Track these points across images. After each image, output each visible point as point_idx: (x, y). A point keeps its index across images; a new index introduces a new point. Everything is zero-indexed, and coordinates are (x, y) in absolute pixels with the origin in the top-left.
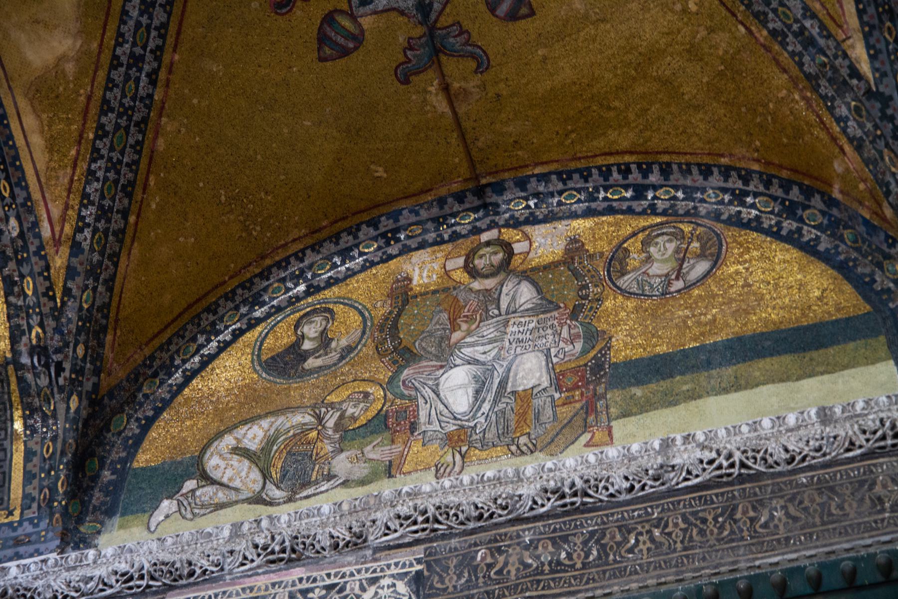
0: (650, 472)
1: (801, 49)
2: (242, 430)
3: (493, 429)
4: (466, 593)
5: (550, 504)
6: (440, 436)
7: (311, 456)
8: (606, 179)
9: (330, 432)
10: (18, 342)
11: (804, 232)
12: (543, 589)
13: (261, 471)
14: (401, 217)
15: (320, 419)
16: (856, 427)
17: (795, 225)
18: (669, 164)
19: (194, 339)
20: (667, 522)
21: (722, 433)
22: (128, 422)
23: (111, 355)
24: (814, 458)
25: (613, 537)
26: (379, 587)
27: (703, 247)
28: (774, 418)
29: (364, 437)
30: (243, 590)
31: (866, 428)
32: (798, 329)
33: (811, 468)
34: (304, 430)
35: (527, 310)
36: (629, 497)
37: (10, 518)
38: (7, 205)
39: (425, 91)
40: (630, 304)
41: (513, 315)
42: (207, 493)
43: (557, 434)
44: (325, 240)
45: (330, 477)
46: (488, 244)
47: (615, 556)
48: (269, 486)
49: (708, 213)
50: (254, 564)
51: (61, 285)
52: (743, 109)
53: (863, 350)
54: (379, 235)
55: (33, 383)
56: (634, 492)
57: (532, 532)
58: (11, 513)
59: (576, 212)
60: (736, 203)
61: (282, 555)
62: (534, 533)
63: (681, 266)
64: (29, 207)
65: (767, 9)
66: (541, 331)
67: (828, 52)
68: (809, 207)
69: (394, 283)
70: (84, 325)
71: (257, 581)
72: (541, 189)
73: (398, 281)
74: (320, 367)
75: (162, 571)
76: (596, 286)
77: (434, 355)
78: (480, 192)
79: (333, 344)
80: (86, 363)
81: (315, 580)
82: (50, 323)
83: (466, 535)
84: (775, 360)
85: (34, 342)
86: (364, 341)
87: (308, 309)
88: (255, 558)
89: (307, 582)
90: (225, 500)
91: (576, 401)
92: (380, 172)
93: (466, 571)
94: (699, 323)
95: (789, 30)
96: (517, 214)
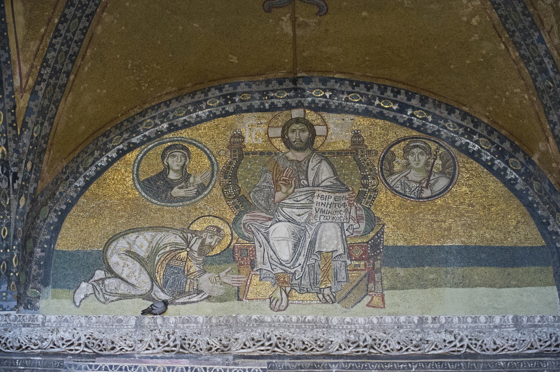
0: (414, 342)
1: (537, 72)
2: (132, 236)
3: (307, 278)
6: (271, 275)
8: (382, 93)
9: (196, 255)
14: (239, 87)
15: (188, 243)
16: (536, 337)
17: (503, 165)
18: (427, 98)
19: (92, 154)
21: (456, 320)
22: (50, 212)
23: (46, 168)
24: (509, 350)
27: (443, 165)
28: (487, 317)
29: (219, 264)
30: (148, 367)
31: (542, 339)
32: (501, 248)
33: (506, 356)
35: (327, 187)
36: (397, 354)
39: (280, 19)
40: (397, 200)
41: (317, 188)
42: (112, 283)
43: (349, 292)
44: (186, 95)
45: (199, 292)
46: (297, 120)
48: (156, 288)
50: (155, 351)
51: (22, 118)
52: (488, 87)
53: (539, 274)
54: (221, 95)
56: (401, 351)
57: (337, 366)
59: (357, 109)
60: (466, 136)
61: (174, 349)
62: (338, 368)
63: (429, 177)
64: (8, 64)
65: (522, 43)
67: (554, 81)
68: (514, 157)
69: (232, 137)
70: (33, 148)
71: (157, 363)
72: (337, 87)
73: (233, 136)
75: (93, 344)
76: (373, 179)
77: (264, 208)
78: (295, 81)
79: (191, 180)
80: (31, 175)
82: (12, 145)
83: (294, 359)
84: (487, 269)
86: (213, 182)
87: (169, 144)
88: (156, 347)
91: (363, 270)
92: (235, 59)
94: (440, 227)
95: (533, 59)
96: (317, 100)
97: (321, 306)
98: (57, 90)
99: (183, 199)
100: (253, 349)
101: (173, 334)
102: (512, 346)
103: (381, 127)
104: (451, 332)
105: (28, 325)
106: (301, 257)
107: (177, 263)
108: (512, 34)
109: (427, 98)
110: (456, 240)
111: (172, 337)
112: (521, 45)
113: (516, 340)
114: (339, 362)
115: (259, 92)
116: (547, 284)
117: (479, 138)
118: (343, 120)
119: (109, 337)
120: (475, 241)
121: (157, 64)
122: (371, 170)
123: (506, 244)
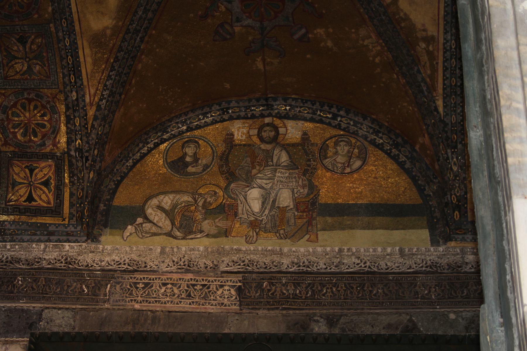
0: (335, 264)
4: (259, 300)
5: (294, 268)
6: (247, 222)
7: (193, 219)
8: (322, 107)
9: (200, 209)
10: (71, 145)
11: (400, 157)
12: (289, 305)
13: (171, 220)
16: (413, 261)
17: (397, 152)
19: (138, 145)
20: (338, 286)
21: (362, 250)
23: (107, 154)
25: (317, 288)
26: (223, 290)
27: (359, 152)
29: (215, 214)
30: (167, 278)
34: (188, 205)
35: (285, 166)
37: (64, 222)
38: (72, 86)
40: (328, 174)
41: (279, 167)
42: (147, 226)
43: (296, 233)
45: (201, 232)
46: (268, 125)
47: (318, 296)
48: (174, 229)
49: (363, 135)
50: (172, 268)
54: (221, 109)
58: (64, 220)
59: (306, 117)
61: (183, 267)
62: (286, 279)
63: (350, 160)
65: (407, 73)
66: (290, 179)
68: (404, 147)
69: (226, 135)
72: (293, 103)
73: (227, 135)
74: (195, 173)
76: (314, 161)
78: (267, 100)
79: (200, 162)
82: (84, 138)
85: (77, 146)
86: (213, 163)
88: (173, 266)
89: (194, 281)
90: (156, 232)
91: (305, 218)
92: (228, 86)
93: (259, 290)
94: (355, 192)
96: (281, 112)
97: (277, 241)
99: (194, 174)
101: (183, 258)
102: (398, 267)
103: (321, 129)
104: (359, 258)
105: (93, 252)
106: (266, 211)
107: (189, 214)
110: (365, 200)
111: (183, 260)
113: (400, 263)
114: (287, 276)
115: (244, 107)
116: (422, 228)
117: (383, 135)
118: (297, 124)
119: (143, 259)
120: (377, 200)
122: (313, 156)
123: (397, 202)
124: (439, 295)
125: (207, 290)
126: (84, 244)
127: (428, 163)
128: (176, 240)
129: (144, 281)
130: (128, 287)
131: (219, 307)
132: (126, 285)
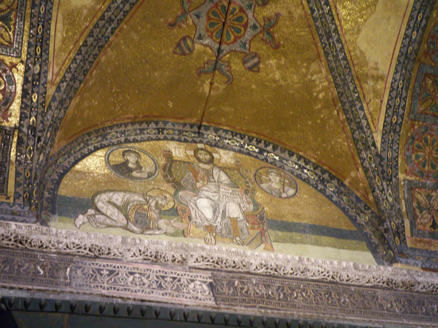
0: (301, 270)
4: (233, 297)
8: (250, 141)
9: (154, 209)
10: (24, 121)
13: (125, 216)
17: (323, 187)
25: (288, 291)
27: (290, 183)
30: (134, 268)
32: (334, 229)
33: (354, 285)
37: (8, 201)
39: (204, 82)
43: (252, 241)
45: (159, 229)
46: (202, 149)
50: (138, 258)
55: (26, 142)
58: (8, 198)
68: (330, 183)
72: (223, 135)
78: (199, 128)
79: (143, 169)
81: (166, 273)
86: (157, 172)
92: (171, 104)
96: (211, 141)
98: (73, 90)
99: (140, 178)
100: (202, 263)
102: (358, 280)
105: (45, 234)
106: (219, 218)
108: (343, 104)
109: (277, 146)
111: (150, 251)
112: (348, 111)
115: (179, 131)
119: (107, 246)
121: (129, 95)
124: (401, 309)
125: (178, 283)
126: (34, 226)
127: (359, 195)
128: (133, 234)
129: (107, 268)
130: (91, 272)
131: (194, 300)
132: (88, 271)
